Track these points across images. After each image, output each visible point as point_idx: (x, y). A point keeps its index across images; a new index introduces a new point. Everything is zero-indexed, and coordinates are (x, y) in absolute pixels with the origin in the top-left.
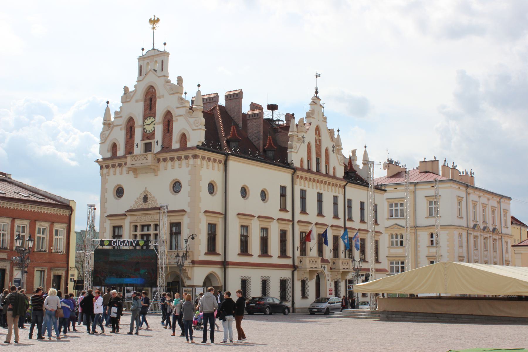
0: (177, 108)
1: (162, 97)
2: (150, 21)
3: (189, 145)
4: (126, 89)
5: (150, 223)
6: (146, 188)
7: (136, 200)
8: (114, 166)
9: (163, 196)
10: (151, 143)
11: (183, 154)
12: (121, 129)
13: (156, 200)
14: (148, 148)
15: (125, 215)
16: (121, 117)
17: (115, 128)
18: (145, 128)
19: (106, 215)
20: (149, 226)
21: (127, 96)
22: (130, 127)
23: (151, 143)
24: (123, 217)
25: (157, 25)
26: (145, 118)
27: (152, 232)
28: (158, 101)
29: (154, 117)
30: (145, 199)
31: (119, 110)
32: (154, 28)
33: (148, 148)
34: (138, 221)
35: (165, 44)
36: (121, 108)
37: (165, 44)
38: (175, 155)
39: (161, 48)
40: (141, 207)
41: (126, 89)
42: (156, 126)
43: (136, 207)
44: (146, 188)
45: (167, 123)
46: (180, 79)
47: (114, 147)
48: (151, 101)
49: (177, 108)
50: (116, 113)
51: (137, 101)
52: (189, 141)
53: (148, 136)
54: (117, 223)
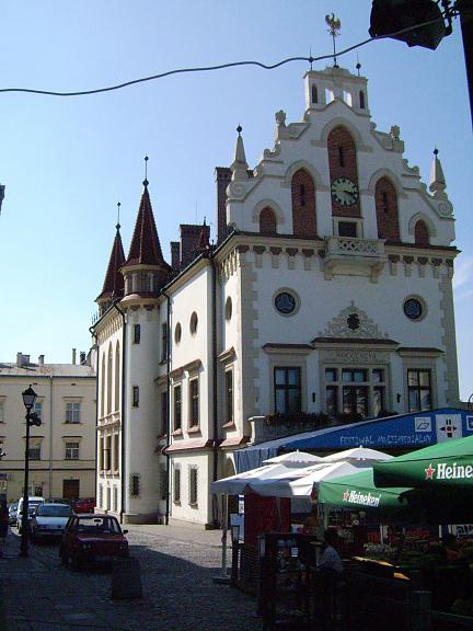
0: (404, 175)
1: (370, 150)
2: (327, 18)
3: (433, 241)
4: (281, 117)
5: (367, 367)
6: (352, 302)
7: (332, 322)
8: (276, 251)
9: (386, 319)
10: (354, 224)
11: (417, 253)
12: (283, 185)
13: (376, 328)
14: (348, 230)
15: (309, 347)
16: (282, 162)
17: (266, 180)
18: (336, 197)
19: (259, 343)
20: (364, 372)
21: (287, 132)
22: (303, 187)
23: (354, 224)
24: (306, 351)
25: (337, 31)
26: (333, 178)
27: (374, 381)
28: (360, 155)
29: (355, 180)
30: (353, 321)
31: (272, 150)
32: (333, 33)
33: (348, 230)
34: (339, 360)
35: (358, 66)
36: (277, 146)
37: (358, 66)
38: (402, 252)
39: (354, 72)
40: (344, 335)
41: (281, 117)
42: (363, 198)
43: (332, 334)
44: (352, 302)
45: (381, 197)
46: (395, 130)
47: (268, 217)
48: (341, 152)
49: (404, 175)
50: (267, 152)
51: (313, 143)
52: (435, 236)
53: (347, 210)
54: (290, 360)
